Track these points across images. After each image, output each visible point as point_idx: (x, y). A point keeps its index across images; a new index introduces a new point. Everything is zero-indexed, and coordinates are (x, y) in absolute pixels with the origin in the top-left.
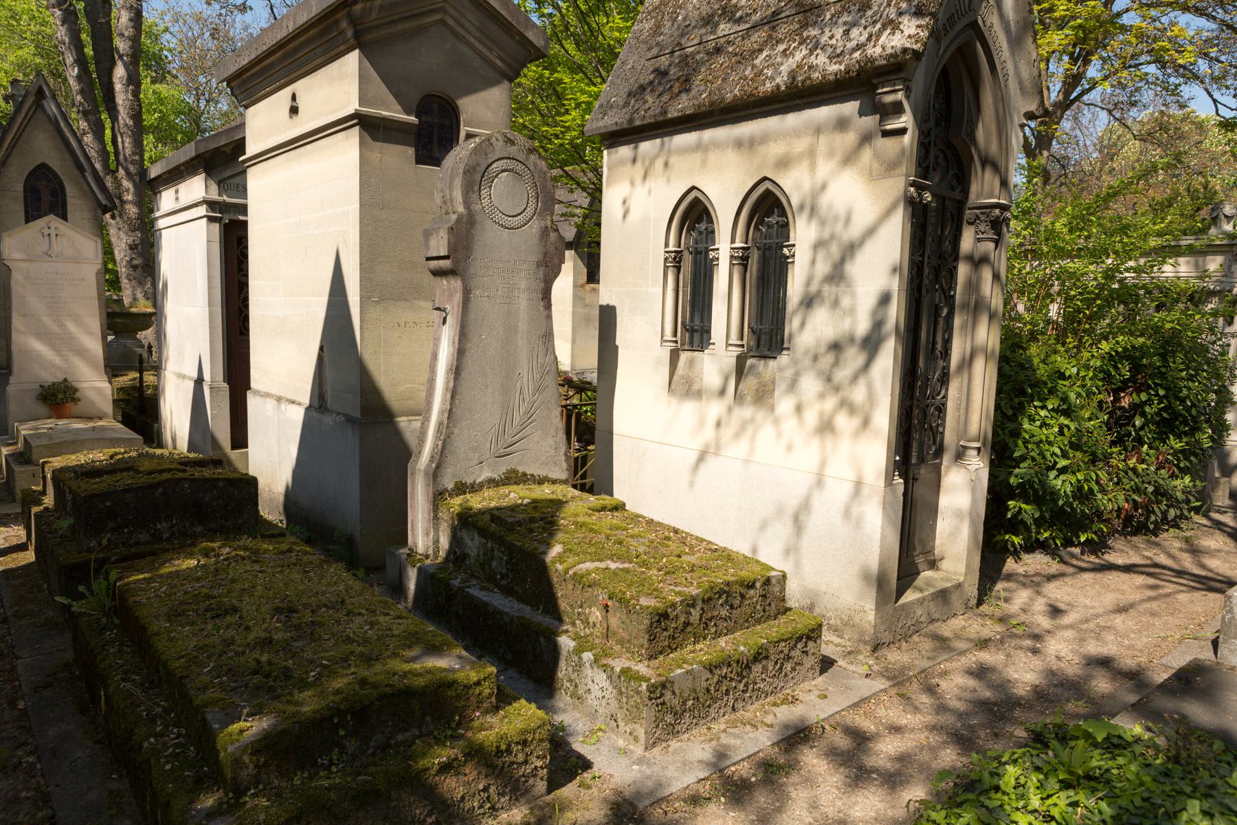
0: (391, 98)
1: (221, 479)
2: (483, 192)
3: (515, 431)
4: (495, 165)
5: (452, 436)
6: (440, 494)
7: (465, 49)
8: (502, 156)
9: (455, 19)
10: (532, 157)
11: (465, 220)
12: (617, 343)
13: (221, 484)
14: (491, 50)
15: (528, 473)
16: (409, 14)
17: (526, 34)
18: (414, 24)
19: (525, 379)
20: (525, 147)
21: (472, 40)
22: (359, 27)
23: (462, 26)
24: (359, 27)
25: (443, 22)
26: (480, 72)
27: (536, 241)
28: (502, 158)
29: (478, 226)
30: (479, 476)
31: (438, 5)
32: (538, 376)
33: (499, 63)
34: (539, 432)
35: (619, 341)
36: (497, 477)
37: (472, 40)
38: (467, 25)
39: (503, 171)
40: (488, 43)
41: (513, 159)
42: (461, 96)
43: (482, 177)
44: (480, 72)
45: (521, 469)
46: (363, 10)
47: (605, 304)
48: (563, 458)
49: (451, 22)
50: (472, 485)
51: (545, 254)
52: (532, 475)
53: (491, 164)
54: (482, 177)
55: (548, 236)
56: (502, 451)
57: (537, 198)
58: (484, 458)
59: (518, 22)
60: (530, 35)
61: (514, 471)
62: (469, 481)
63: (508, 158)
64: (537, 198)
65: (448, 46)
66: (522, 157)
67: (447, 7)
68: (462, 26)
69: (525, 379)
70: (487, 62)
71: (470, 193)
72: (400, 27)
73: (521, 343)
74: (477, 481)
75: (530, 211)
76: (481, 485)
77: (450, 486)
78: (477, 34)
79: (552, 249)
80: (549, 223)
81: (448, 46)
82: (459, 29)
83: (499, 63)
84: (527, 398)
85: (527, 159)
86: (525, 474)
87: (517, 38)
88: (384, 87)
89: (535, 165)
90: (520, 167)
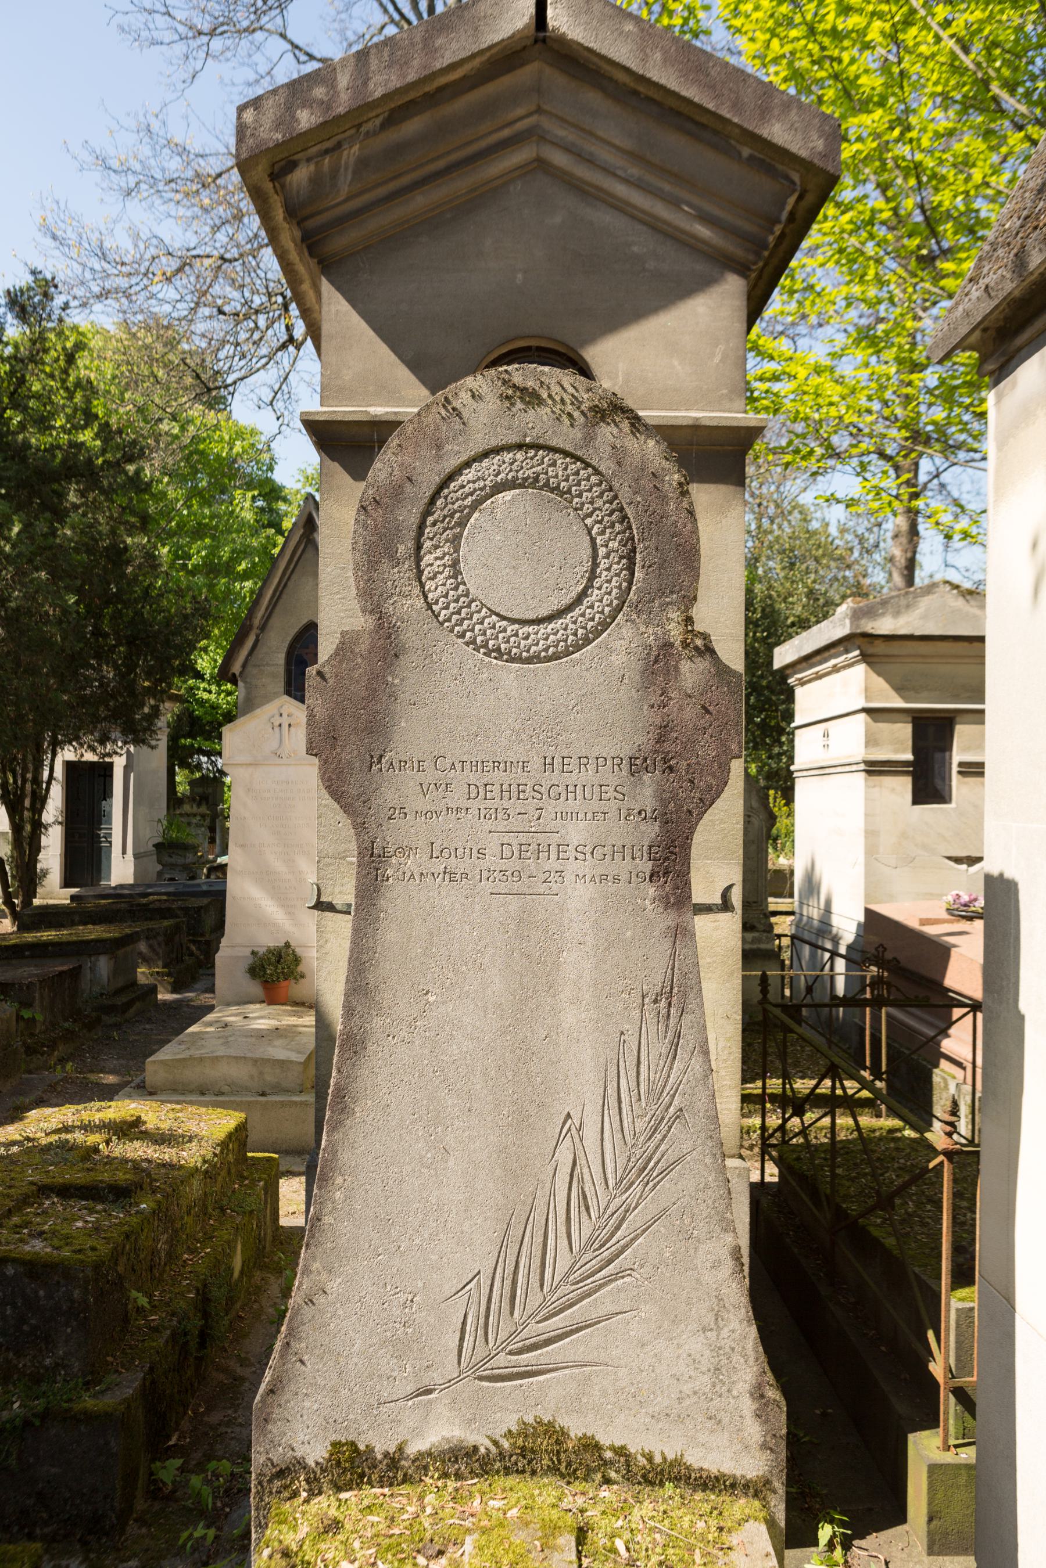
0: (403, 373)
1: (14, 1260)
2: (428, 559)
3: (556, 1300)
4: (469, 474)
5: (320, 1300)
6: (281, 1474)
7: (604, 217)
8: (494, 443)
9: (568, 149)
10: (607, 432)
11: (364, 646)
12: (1023, 1006)
13: (10, 1271)
14: (675, 203)
15: (604, 1440)
16: (441, 164)
17: (764, 132)
18: (460, 185)
19: (591, 1134)
20: (577, 402)
21: (621, 190)
22: (311, 224)
23: (590, 161)
24: (311, 224)
25: (541, 165)
26: (651, 265)
27: (628, 693)
28: (497, 451)
29: (409, 662)
30: (418, 1432)
31: (520, 126)
32: (640, 1125)
33: (703, 231)
34: (647, 1309)
35: (1026, 1003)
36: (484, 1444)
37: (621, 190)
38: (605, 155)
39: (499, 488)
40: (667, 187)
41: (537, 447)
42: (592, 339)
43: (427, 512)
44: (651, 265)
45: (576, 1427)
46: (315, 180)
47: (995, 872)
48: (748, 1406)
49: (559, 159)
50: (393, 1461)
51: (663, 732)
52: (621, 1451)
53: (458, 471)
54: (427, 512)
55: (671, 672)
56: (502, 1359)
57: (630, 558)
58: (436, 1377)
59: (737, 105)
60: (777, 132)
61: (555, 1434)
62: (382, 1444)
63: (520, 446)
64: (630, 558)
65: (558, 219)
66: (568, 436)
67: (546, 123)
68: (590, 161)
69: (591, 1134)
70: (684, 244)
71: (385, 565)
72: (420, 201)
73: (569, 1018)
74: (412, 1450)
75: (603, 598)
76: (423, 1462)
77: (315, 1453)
78: (634, 171)
79: (690, 713)
80: (675, 633)
81: (558, 219)
82: (583, 172)
83: (703, 231)
84: (598, 1197)
85: (589, 439)
86: (591, 1446)
87: (746, 152)
88: (384, 350)
89: (619, 455)
90: (560, 470)
